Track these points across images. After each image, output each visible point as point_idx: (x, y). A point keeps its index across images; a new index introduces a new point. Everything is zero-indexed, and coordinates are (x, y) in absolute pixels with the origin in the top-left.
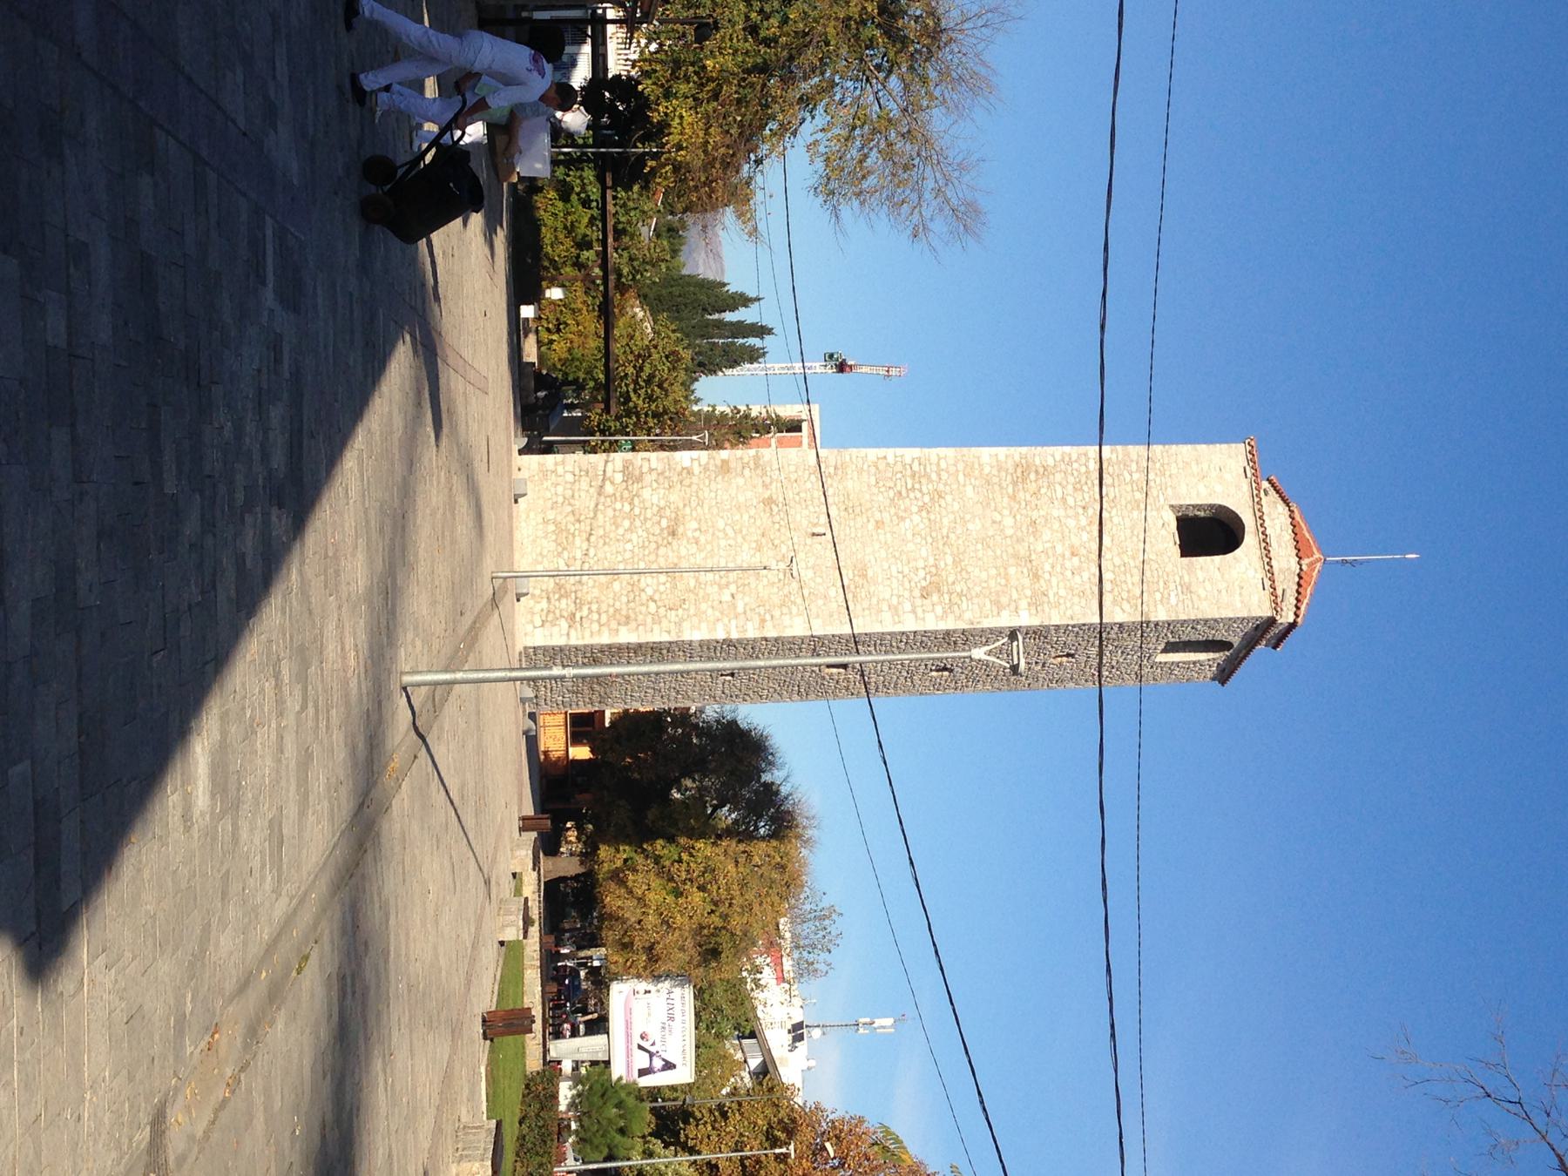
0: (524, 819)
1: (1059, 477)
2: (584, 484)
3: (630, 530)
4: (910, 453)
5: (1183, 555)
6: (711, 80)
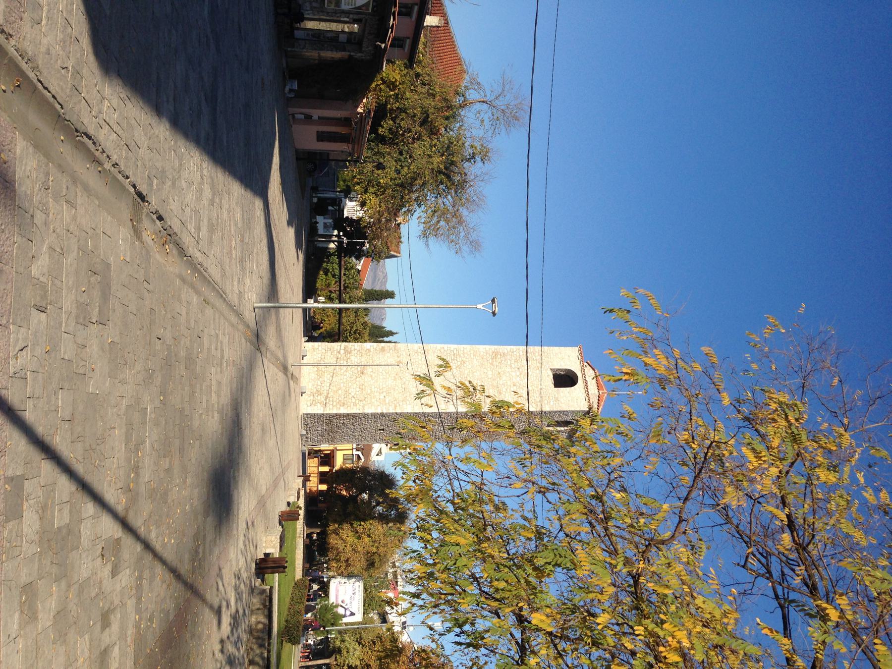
1: (509, 357)
2: (329, 353)
6: (382, 187)
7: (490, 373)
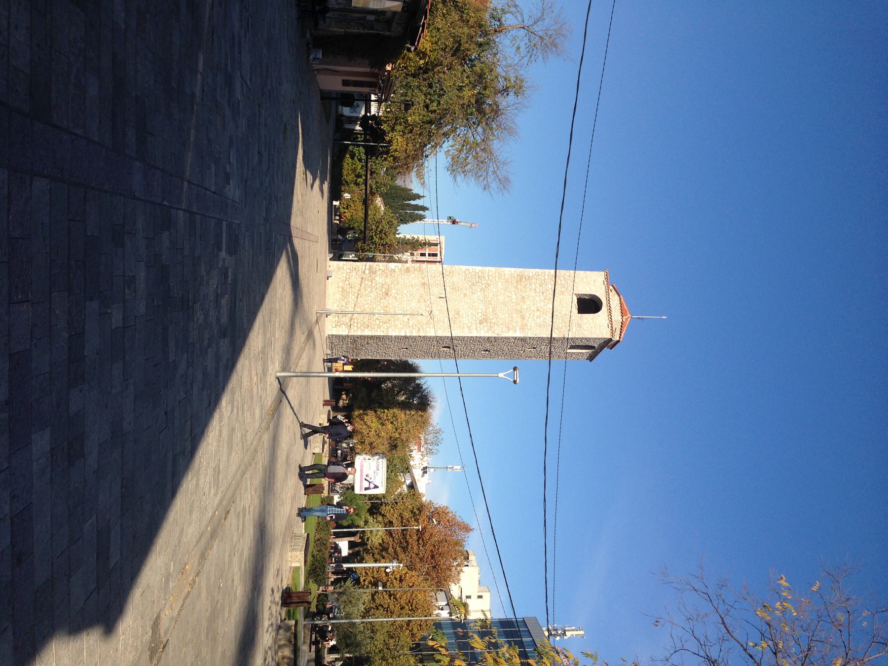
0: (325, 401)
1: (534, 281)
2: (354, 274)
3: (371, 292)
4: (478, 269)
5: (579, 312)
7: (514, 296)
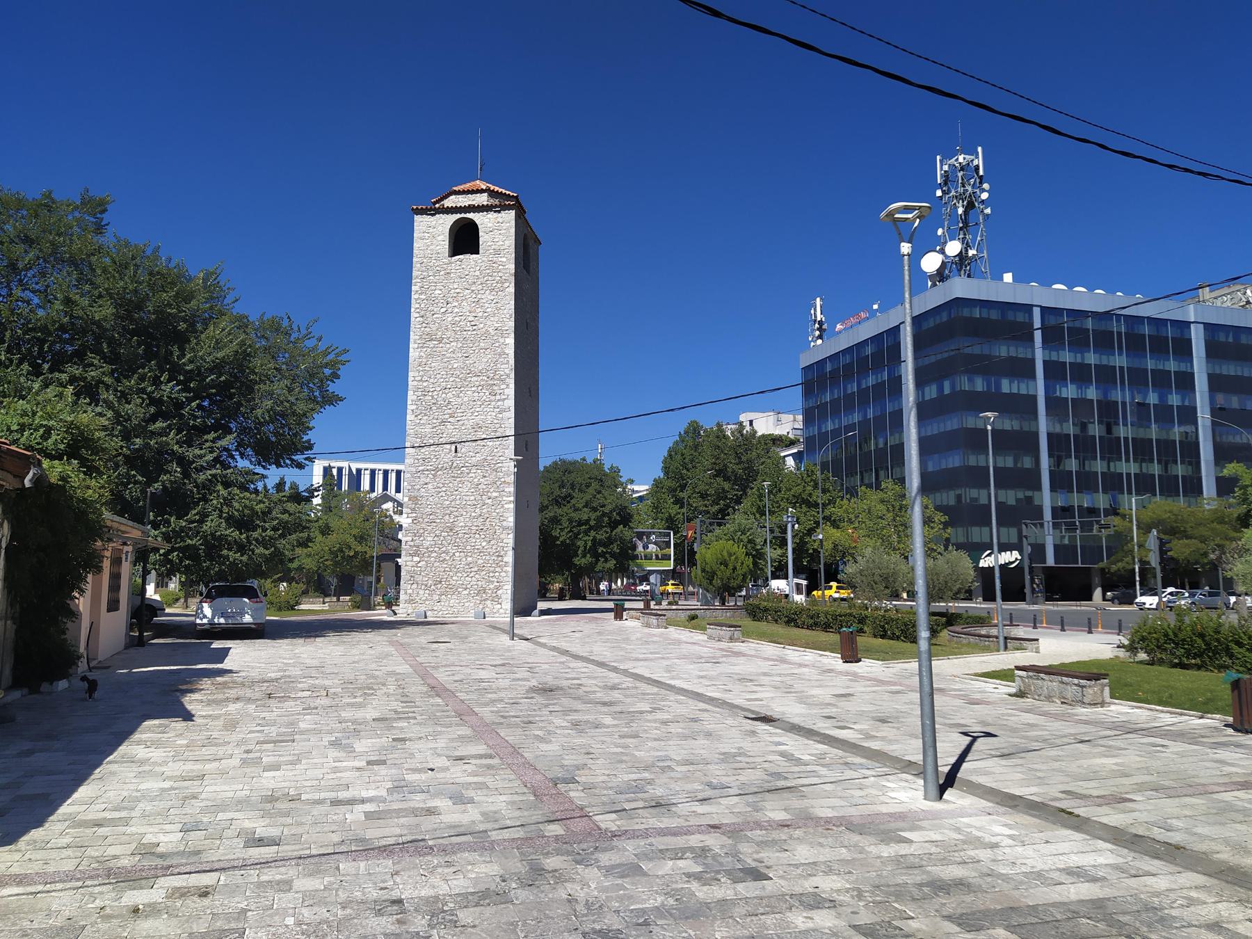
0: (616, 618)
4: (411, 396)
